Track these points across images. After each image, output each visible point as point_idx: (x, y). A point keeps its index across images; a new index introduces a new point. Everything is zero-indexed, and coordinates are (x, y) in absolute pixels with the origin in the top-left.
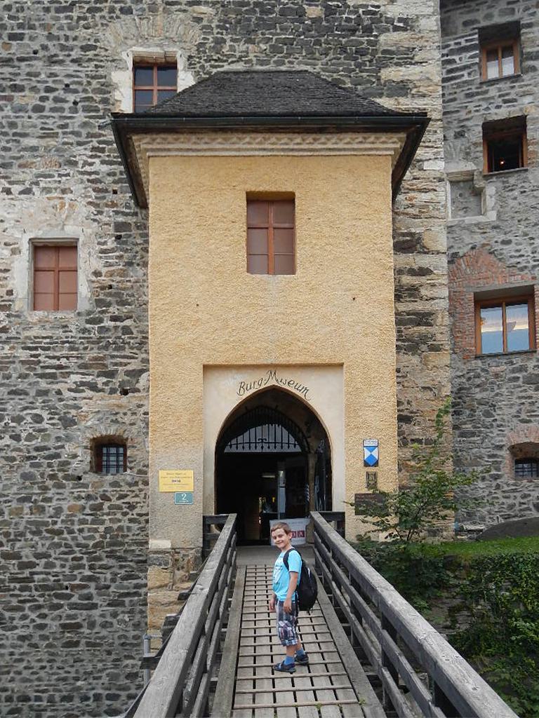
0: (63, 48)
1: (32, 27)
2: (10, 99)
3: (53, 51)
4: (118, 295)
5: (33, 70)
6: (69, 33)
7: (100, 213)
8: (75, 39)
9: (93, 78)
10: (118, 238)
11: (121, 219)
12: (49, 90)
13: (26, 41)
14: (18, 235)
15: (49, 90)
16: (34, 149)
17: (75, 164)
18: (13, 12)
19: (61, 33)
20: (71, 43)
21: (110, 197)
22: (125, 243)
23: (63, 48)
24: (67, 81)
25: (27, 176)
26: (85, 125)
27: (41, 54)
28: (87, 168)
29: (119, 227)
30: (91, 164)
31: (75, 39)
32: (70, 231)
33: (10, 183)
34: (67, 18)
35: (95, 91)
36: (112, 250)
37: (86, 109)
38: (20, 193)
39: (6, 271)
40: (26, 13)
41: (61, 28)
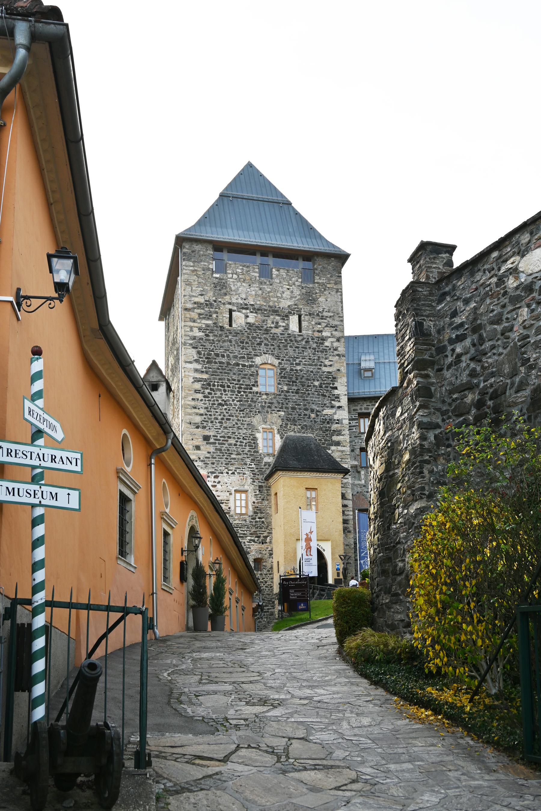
0: (242, 424)
1: (233, 416)
2: (227, 441)
3: (239, 425)
4: (260, 510)
5: (234, 431)
6: (244, 419)
7: (254, 482)
8: (245, 421)
9: (251, 435)
10: (260, 490)
11: (260, 484)
12: (238, 438)
13: (231, 421)
14: (231, 488)
15: (238, 438)
16: (234, 459)
17: (247, 464)
18: (227, 411)
19: (241, 419)
20: (244, 423)
21: (257, 476)
22: (262, 492)
23: (242, 424)
24: (244, 436)
25: (232, 468)
26: (249, 451)
27: (236, 426)
28: (250, 466)
29: (260, 487)
30: (251, 465)
31: (245, 421)
32: (246, 488)
33: (228, 470)
34: (243, 414)
35: (252, 440)
36: (258, 495)
37: (249, 446)
38: (232, 474)
39: (228, 500)
40: (231, 411)
41: (241, 417)
